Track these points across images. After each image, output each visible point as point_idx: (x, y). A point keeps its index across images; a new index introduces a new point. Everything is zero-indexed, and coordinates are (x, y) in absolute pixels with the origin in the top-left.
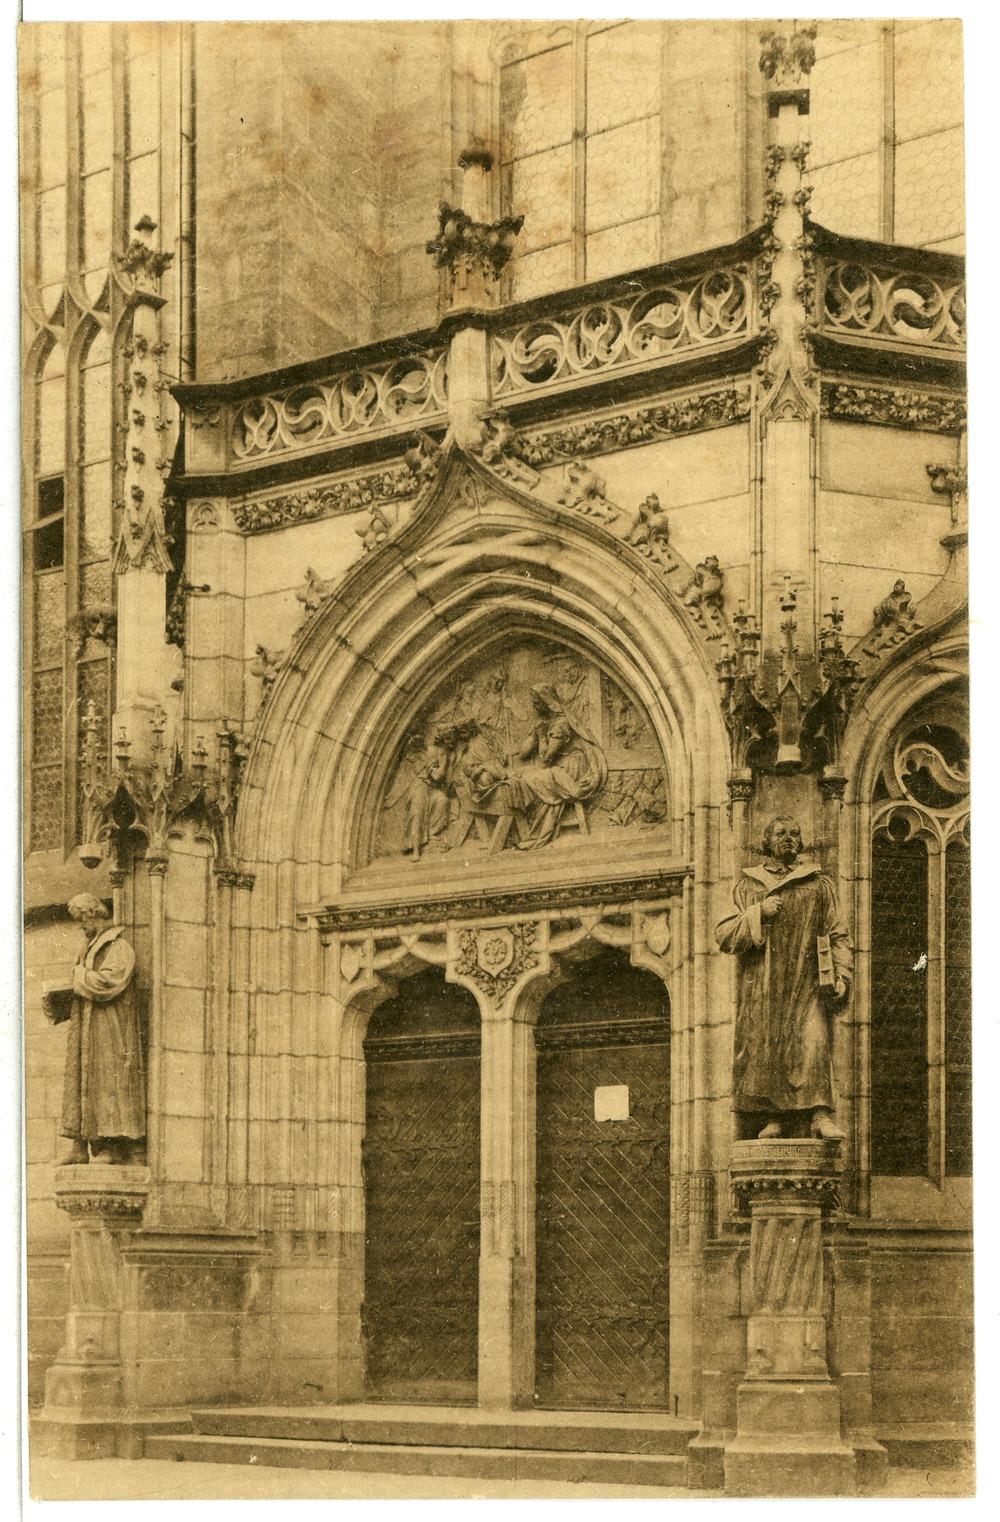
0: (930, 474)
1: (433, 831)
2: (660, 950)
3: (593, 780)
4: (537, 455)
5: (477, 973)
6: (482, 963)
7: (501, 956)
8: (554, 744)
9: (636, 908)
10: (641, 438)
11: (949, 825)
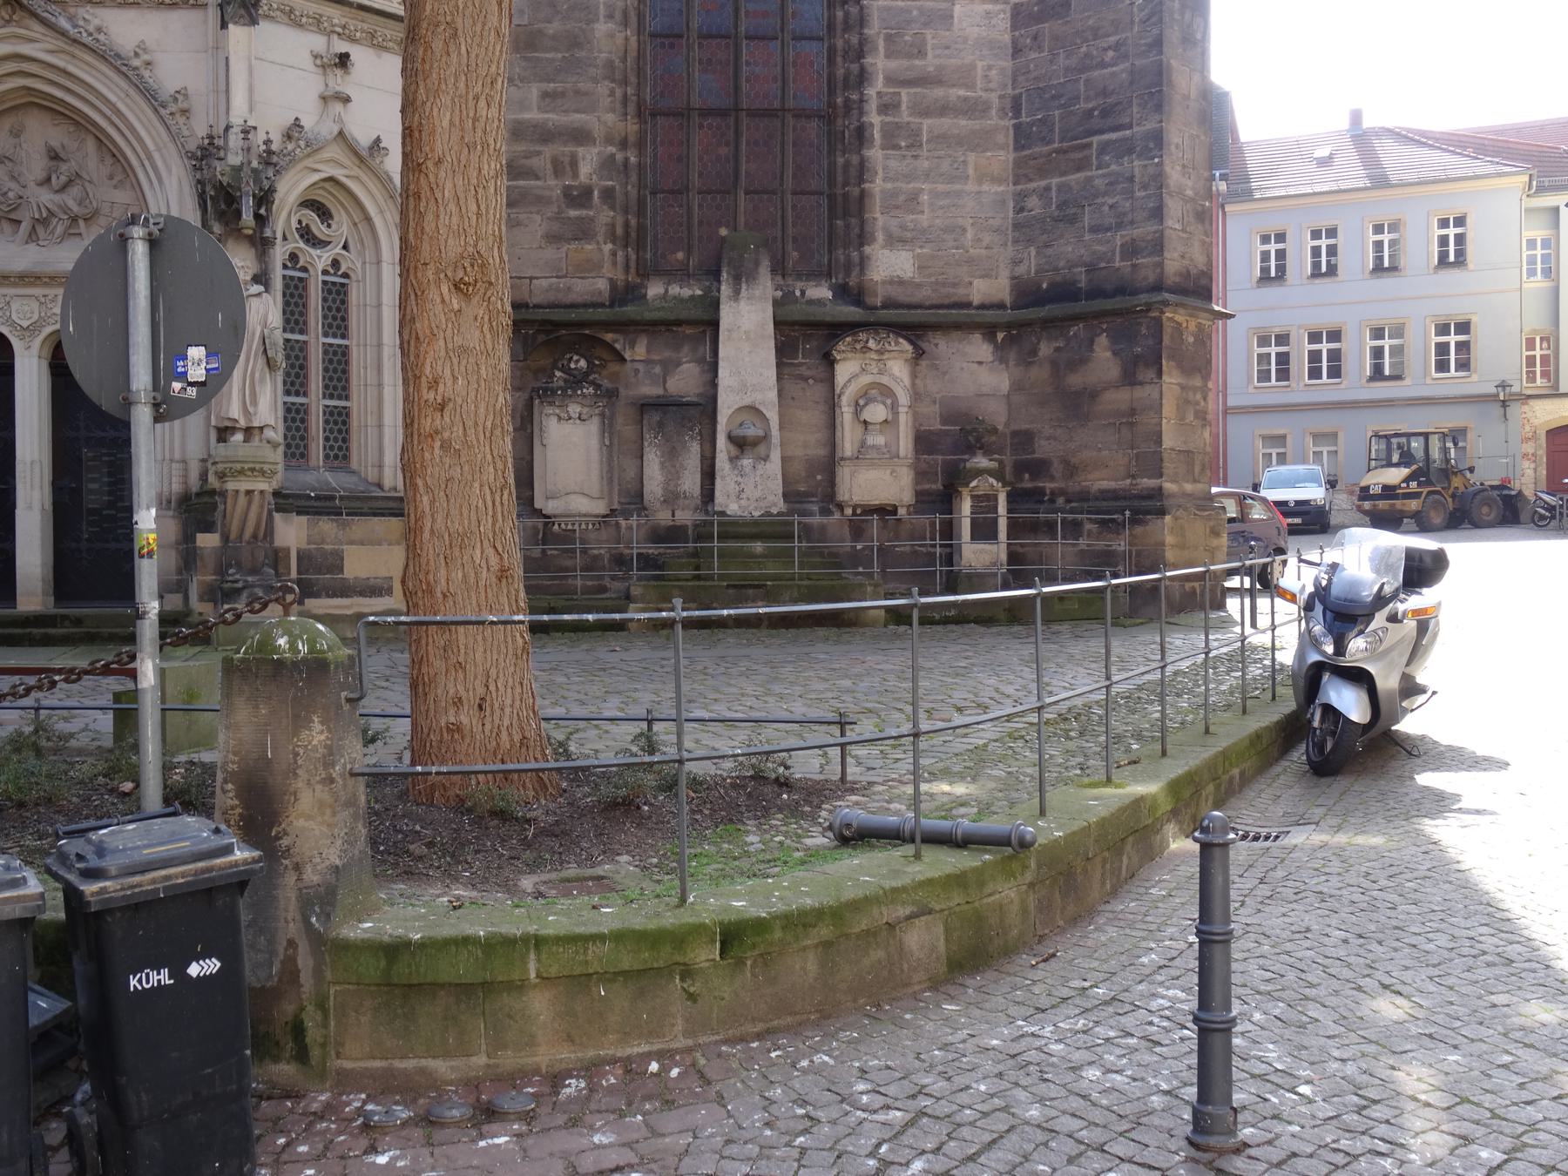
5: (13, 324)
6: (14, 317)
7: (28, 315)
8: (63, 179)
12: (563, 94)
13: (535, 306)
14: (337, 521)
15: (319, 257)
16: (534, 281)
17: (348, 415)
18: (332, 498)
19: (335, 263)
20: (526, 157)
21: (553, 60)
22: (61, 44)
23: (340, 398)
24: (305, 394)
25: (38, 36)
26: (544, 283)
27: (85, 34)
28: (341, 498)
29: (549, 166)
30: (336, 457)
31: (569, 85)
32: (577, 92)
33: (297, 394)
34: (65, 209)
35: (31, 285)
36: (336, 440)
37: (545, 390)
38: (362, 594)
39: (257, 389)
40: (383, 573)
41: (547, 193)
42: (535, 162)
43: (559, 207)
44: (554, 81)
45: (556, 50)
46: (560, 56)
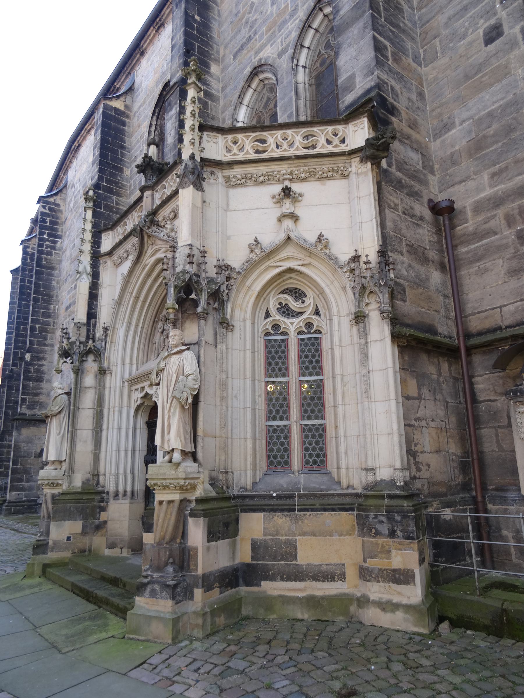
12: (506, 168)
13: (507, 327)
14: (290, 516)
15: (292, 323)
16: (504, 309)
20: (485, 223)
21: (496, 150)
23: (317, 418)
24: (288, 419)
26: (511, 307)
28: (300, 496)
29: (503, 222)
30: (315, 462)
31: (510, 160)
32: (517, 162)
33: (281, 419)
36: (314, 449)
37: (515, 392)
38: (315, 578)
40: (335, 560)
41: (504, 241)
42: (492, 224)
43: (515, 248)
44: (498, 163)
45: (497, 142)
46: (500, 144)
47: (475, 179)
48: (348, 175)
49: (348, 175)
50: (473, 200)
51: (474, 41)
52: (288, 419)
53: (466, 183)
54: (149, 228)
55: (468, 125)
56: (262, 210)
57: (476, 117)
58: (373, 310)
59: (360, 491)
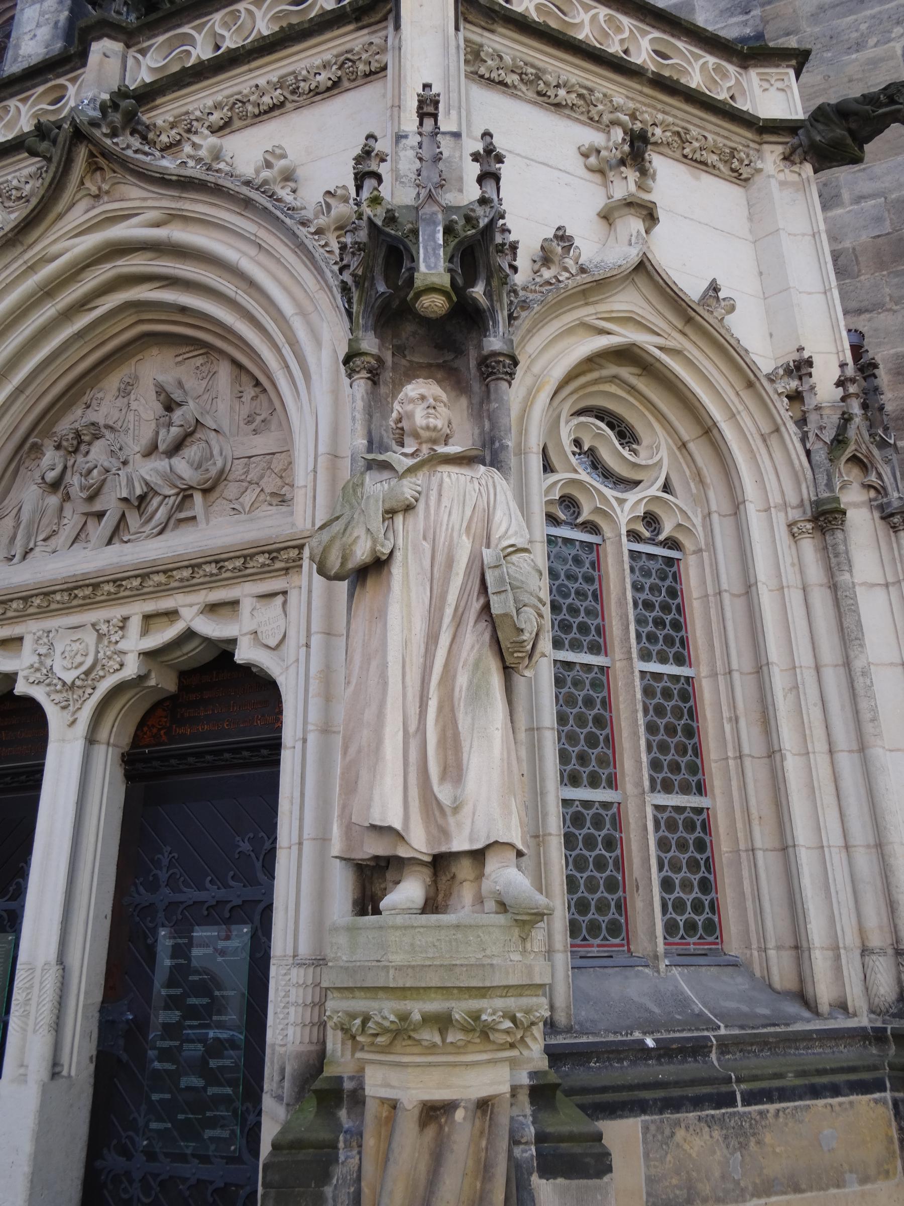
0: (583, 155)
1: (41, 537)
2: (273, 643)
3: (213, 472)
4: (164, 138)
7: (79, 659)
9: (245, 591)
10: (273, 108)
11: (628, 506)
14: (721, 1122)
15: (621, 502)
17: (706, 827)
18: (698, 1049)
19: (651, 520)
22: (168, 201)
23: (685, 789)
24: (612, 783)
25: (137, 204)
27: (191, 163)
28: (724, 1045)
30: (691, 927)
33: (594, 782)
34: (171, 477)
35: (89, 604)
39: (464, 722)
47: (895, 311)
48: (746, 180)
49: (746, 180)
50: (892, 351)
51: (882, 60)
52: (612, 783)
53: (874, 314)
54: (114, 134)
55: (874, 206)
56: (557, 173)
57: (893, 196)
58: (856, 505)
59: (864, 1021)
